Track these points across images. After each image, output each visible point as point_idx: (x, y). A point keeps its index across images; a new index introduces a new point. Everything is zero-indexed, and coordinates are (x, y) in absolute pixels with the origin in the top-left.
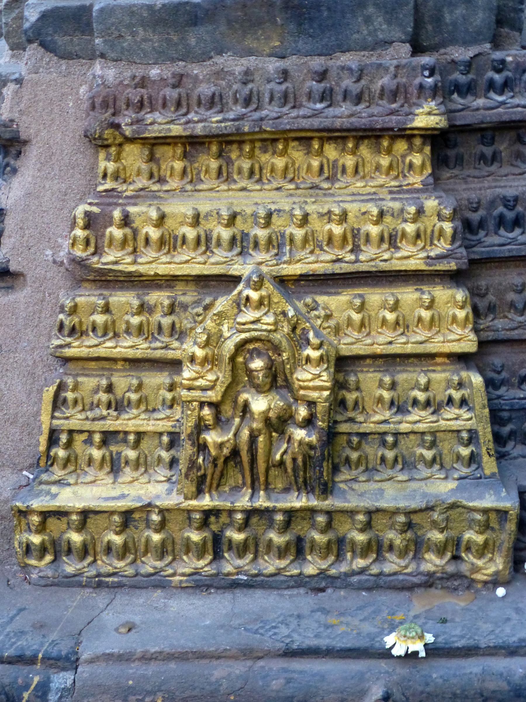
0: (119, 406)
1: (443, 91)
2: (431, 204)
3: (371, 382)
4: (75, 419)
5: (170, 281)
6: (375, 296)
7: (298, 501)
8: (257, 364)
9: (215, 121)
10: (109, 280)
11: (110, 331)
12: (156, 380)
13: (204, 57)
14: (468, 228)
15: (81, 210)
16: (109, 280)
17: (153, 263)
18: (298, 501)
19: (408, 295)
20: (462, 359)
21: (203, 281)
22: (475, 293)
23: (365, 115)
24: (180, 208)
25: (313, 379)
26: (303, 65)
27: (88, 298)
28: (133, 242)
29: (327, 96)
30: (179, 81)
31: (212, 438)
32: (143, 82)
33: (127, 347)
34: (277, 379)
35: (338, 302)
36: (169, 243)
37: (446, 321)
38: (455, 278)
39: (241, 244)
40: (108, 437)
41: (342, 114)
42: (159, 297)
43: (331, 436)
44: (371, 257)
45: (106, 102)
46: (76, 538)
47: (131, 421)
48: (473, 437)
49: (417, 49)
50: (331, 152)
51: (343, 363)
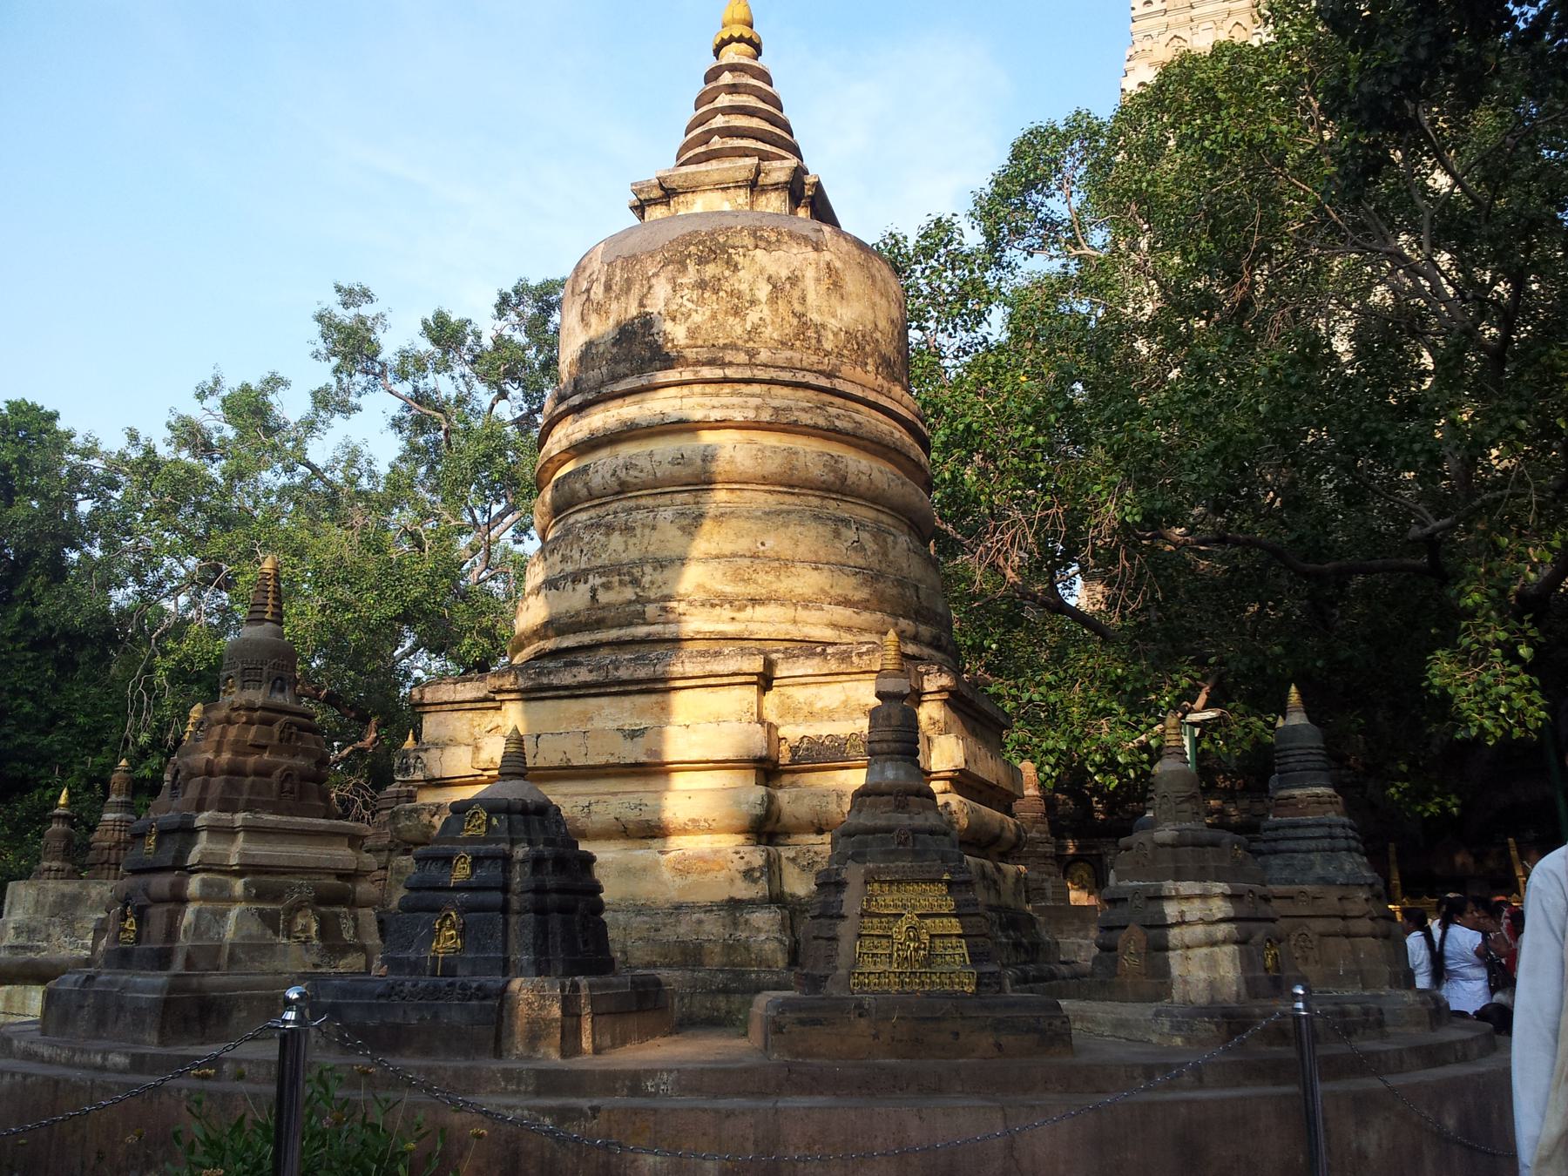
12: (884, 941)
20: (959, 936)
21: (894, 915)
23: (931, 876)
25: (925, 938)
34: (917, 939)
36: (887, 906)
37: (954, 926)
38: (955, 916)
39: (904, 907)
41: (927, 876)
45: (869, 872)
51: (932, 936)
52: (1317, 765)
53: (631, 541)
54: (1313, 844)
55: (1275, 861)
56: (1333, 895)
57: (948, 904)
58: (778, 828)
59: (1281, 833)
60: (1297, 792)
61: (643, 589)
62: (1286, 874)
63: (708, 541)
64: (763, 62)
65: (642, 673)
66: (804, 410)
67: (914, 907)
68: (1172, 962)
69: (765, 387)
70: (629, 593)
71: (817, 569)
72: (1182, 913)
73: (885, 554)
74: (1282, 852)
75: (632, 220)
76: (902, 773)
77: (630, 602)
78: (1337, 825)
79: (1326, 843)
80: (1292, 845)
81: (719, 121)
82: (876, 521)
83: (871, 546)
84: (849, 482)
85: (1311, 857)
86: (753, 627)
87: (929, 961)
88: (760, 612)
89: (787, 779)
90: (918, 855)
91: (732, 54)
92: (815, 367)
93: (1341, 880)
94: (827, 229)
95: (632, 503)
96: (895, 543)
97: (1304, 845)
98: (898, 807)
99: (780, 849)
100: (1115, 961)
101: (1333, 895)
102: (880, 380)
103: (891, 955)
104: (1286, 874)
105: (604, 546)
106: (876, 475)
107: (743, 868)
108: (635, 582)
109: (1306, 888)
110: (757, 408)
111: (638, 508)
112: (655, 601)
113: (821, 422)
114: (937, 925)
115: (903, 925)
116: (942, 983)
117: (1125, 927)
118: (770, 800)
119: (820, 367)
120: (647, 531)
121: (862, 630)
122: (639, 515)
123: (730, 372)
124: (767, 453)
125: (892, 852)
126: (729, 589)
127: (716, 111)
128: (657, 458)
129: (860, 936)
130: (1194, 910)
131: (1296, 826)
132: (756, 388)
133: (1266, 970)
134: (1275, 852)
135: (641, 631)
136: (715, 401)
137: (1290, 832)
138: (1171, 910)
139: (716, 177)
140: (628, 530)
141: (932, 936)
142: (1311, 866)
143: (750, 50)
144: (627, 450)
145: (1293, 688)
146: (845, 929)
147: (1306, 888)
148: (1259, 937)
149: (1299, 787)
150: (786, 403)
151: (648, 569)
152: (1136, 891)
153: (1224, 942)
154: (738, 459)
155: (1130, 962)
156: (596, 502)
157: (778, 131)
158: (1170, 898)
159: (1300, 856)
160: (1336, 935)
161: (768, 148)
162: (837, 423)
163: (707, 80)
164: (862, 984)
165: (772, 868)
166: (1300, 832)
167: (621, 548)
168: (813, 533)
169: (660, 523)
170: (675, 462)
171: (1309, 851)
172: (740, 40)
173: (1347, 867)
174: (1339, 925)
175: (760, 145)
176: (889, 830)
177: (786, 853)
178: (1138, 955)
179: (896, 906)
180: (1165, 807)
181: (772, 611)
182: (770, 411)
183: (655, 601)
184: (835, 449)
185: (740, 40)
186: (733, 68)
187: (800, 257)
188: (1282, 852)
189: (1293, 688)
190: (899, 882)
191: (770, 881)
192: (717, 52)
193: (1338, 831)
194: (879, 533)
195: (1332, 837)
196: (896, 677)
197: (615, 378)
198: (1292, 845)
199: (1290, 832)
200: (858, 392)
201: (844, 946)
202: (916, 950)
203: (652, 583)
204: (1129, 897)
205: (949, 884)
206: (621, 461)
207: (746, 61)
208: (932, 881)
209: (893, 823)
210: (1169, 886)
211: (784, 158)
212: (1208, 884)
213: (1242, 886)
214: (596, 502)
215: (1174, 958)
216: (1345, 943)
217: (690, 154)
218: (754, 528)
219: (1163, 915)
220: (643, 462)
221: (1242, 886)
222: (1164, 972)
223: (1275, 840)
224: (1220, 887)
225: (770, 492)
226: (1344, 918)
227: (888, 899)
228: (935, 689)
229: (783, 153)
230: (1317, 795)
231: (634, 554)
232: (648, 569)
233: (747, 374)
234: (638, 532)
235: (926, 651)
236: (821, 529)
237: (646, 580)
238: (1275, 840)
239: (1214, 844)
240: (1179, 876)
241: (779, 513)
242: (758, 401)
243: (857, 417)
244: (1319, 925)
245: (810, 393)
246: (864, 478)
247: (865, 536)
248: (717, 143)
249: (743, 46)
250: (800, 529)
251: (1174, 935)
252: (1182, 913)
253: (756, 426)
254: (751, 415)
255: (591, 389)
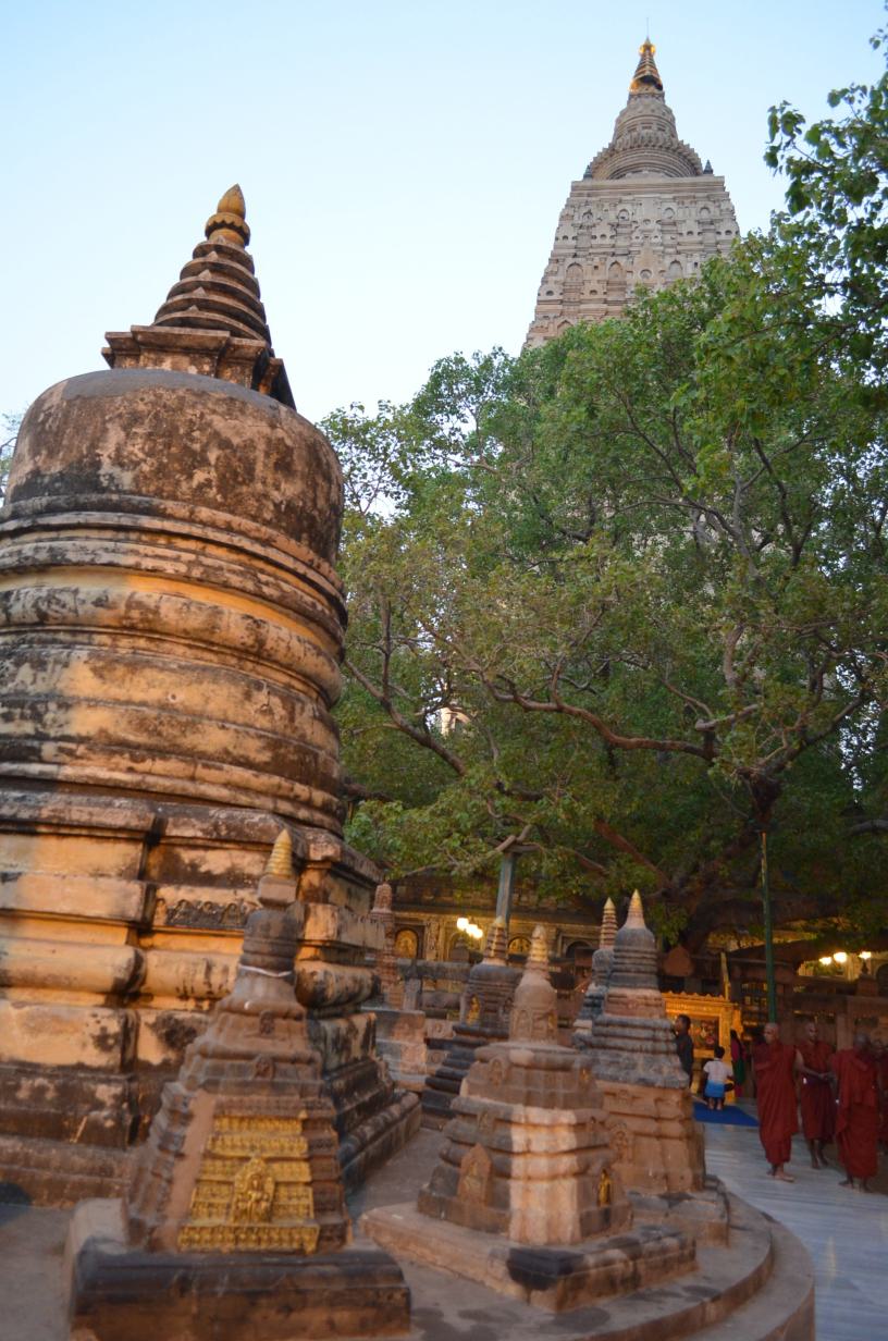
0: (214, 1195)
1: (307, 1108)
2: (302, 1139)
3: (283, 1191)
4: (201, 1199)
5: (231, 1158)
6: (286, 1165)
7: (262, 1225)
8: (255, 1183)
9: (250, 1113)
10: (215, 1157)
11: (214, 1173)
12: (225, 1189)
13: (248, 1094)
14: (310, 1147)
15: (210, 1137)
16: (215, 1157)
17: (230, 1153)
18: (262, 1225)
19: (294, 1165)
22: (311, 1167)
24: (237, 1138)
25: (270, 1187)
26: (273, 1099)
27: (209, 1162)
28: (224, 1146)
29: (278, 1108)
30: (241, 1101)
31: (240, 1204)
32: (231, 1101)
33: (219, 1177)
34: (260, 1188)
35: (276, 1166)
36: (233, 1147)
37: (303, 1172)
39: (253, 1148)
40: (210, 1205)
41: (282, 1113)
42: (228, 1163)
43: (272, 1205)
44: (287, 1153)
46: (197, 1237)
47: (216, 1201)
48: (308, 1207)
49: (302, 1096)
50: (277, 1123)
52: (649, 969)
53: (41, 675)
54: (637, 1044)
55: (603, 1057)
56: (650, 1101)
57: (300, 1147)
58: (143, 989)
59: (610, 1029)
60: (629, 993)
61: (44, 726)
62: (611, 1071)
63: (119, 686)
64: (249, 250)
65: (25, 814)
66: (234, 572)
67: (263, 1149)
68: (513, 1192)
69: (200, 545)
70: (29, 728)
71: (223, 727)
72: (529, 1142)
73: (292, 720)
74: (611, 1048)
75: (104, 366)
76: (272, 993)
77: (28, 737)
78: (660, 1029)
79: (649, 1045)
80: (619, 1042)
81: (200, 293)
82: (288, 686)
83: (280, 711)
84: (268, 646)
85: (635, 1056)
86: (150, 779)
87: (269, 1215)
88: (159, 765)
89: (158, 940)
90: (277, 1088)
91: (221, 236)
92: (253, 534)
93: (658, 1084)
94: (283, 409)
95: (49, 636)
96: (303, 709)
97: (630, 1044)
98: (262, 1031)
99: (142, 1012)
100: (457, 1178)
101: (652, 1095)
102: (312, 555)
103: (229, 1206)
104: (611, 1071)
105: (14, 675)
106: (295, 643)
107: (97, 1032)
108: (37, 717)
109: (628, 1087)
110: (190, 564)
111: (54, 641)
112: (56, 739)
113: (250, 585)
114: (284, 1171)
115: (249, 1171)
116: (281, 1240)
117: (472, 1145)
118: (138, 962)
119: (257, 534)
120: (58, 667)
121: (259, 793)
122: (53, 651)
123: (168, 525)
124: (193, 609)
125: (246, 1084)
126: (131, 738)
127: (199, 284)
128: (81, 596)
129: (198, 1181)
130: (540, 1142)
131: (623, 1025)
132: (192, 545)
133: (598, 1202)
134: (604, 1047)
135: (34, 768)
136: (149, 550)
137: (619, 1030)
138: (518, 1137)
139: (185, 343)
140: (40, 664)
141: (277, 1184)
142: (634, 1066)
143: (239, 237)
144: (53, 583)
145: (636, 895)
146: (183, 1172)
147: (628, 1087)
148: (596, 1168)
149: (630, 987)
150: (217, 563)
151: (52, 706)
152: (485, 1110)
153: (564, 1176)
154: (163, 611)
155: (472, 1185)
156: (13, 629)
157: (252, 313)
158: (518, 1124)
159: (625, 1054)
160: (648, 1135)
161: (241, 326)
162: (266, 590)
163: (196, 255)
164: (191, 1241)
165: (128, 1034)
166: (627, 1031)
167: (29, 680)
168: (225, 692)
169: (74, 663)
170: (99, 603)
171: (633, 1051)
172: (231, 226)
173: (666, 1070)
174: (652, 1127)
175: (228, 320)
176: (248, 1057)
177: (148, 1017)
178: (481, 1179)
179: (243, 1147)
180: (522, 1021)
181: (173, 765)
182: (201, 569)
183: (56, 739)
184: (260, 611)
185: (231, 226)
186: (219, 249)
187: (255, 429)
188: (611, 1048)
189: (636, 895)
190: (251, 1118)
191: (123, 1051)
192: (209, 231)
193: (661, 1035)
194: (289, 700)
195: (655, 1039)
196: (278, 883)
197: (52, 510)
198: (619, 1042)
199: (619, 1030)
200: (289, 563)
201: (179, 1191)
202: (258, 1201)
203: (54, 721)
204: (479, 1114)
205: (304, 1122)
206: (44, 593)
207: (233, 246)
208: (287, 1119)
209: (253, 1049)
210: (519, 1111)
211: (254, 338)
212: (556, 1112)
213: (587, 1113)
214: (13, 629)
215: (515, 1188)
216: (656, 1142)
217: (167, 317)
218: (168, 680)
219: (510, 1144)
220: (67, 598)
221: (587, 1113)
222: (500, 1200)
223: (606, 1036)
224: (568, 1117)
225: (190, 646)
226: (658, 1119)
227: (237, 1139)
228: (319, 858)
229: (246, 329)
230: (646, 998)
231: (40, 688)
232: (52, 706)
233: (185, 529)
234: (50, 667)
235: (318, 816)
236: (233, 689)
237: (48, 717)
238: (606, 1036)
239: (565, 1068)
240: (529, 1101)
241: (193, 669)
242: (192, 557)
243: (285, 587)
244: (635, 1125)
245: (243, 558)
246: (283, 645)
247: (275, 701)
248: (193, 312)
249: (232, 233)
250: (212, 687)
251: (518, 1165)
252: (529, 1142)
253: (186, 578)
254: (183, 569)
255: (28, 517)
